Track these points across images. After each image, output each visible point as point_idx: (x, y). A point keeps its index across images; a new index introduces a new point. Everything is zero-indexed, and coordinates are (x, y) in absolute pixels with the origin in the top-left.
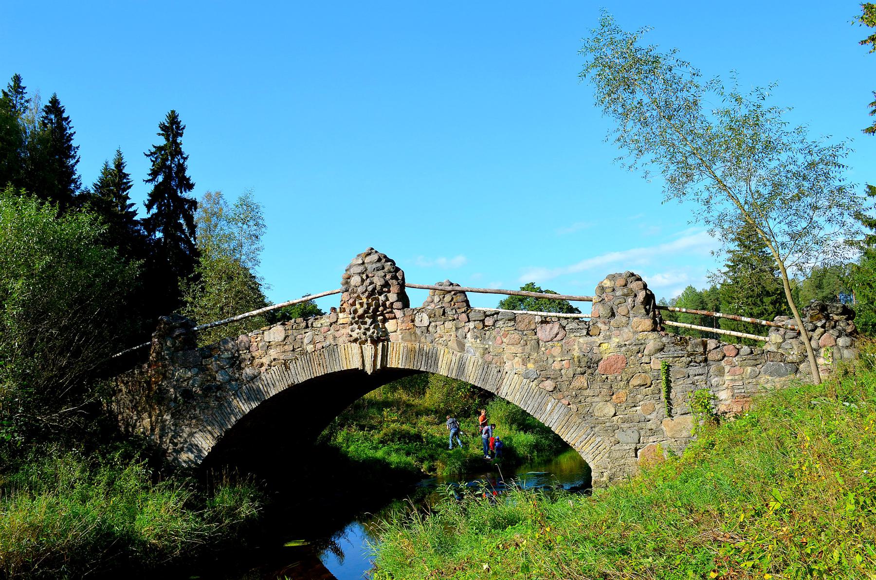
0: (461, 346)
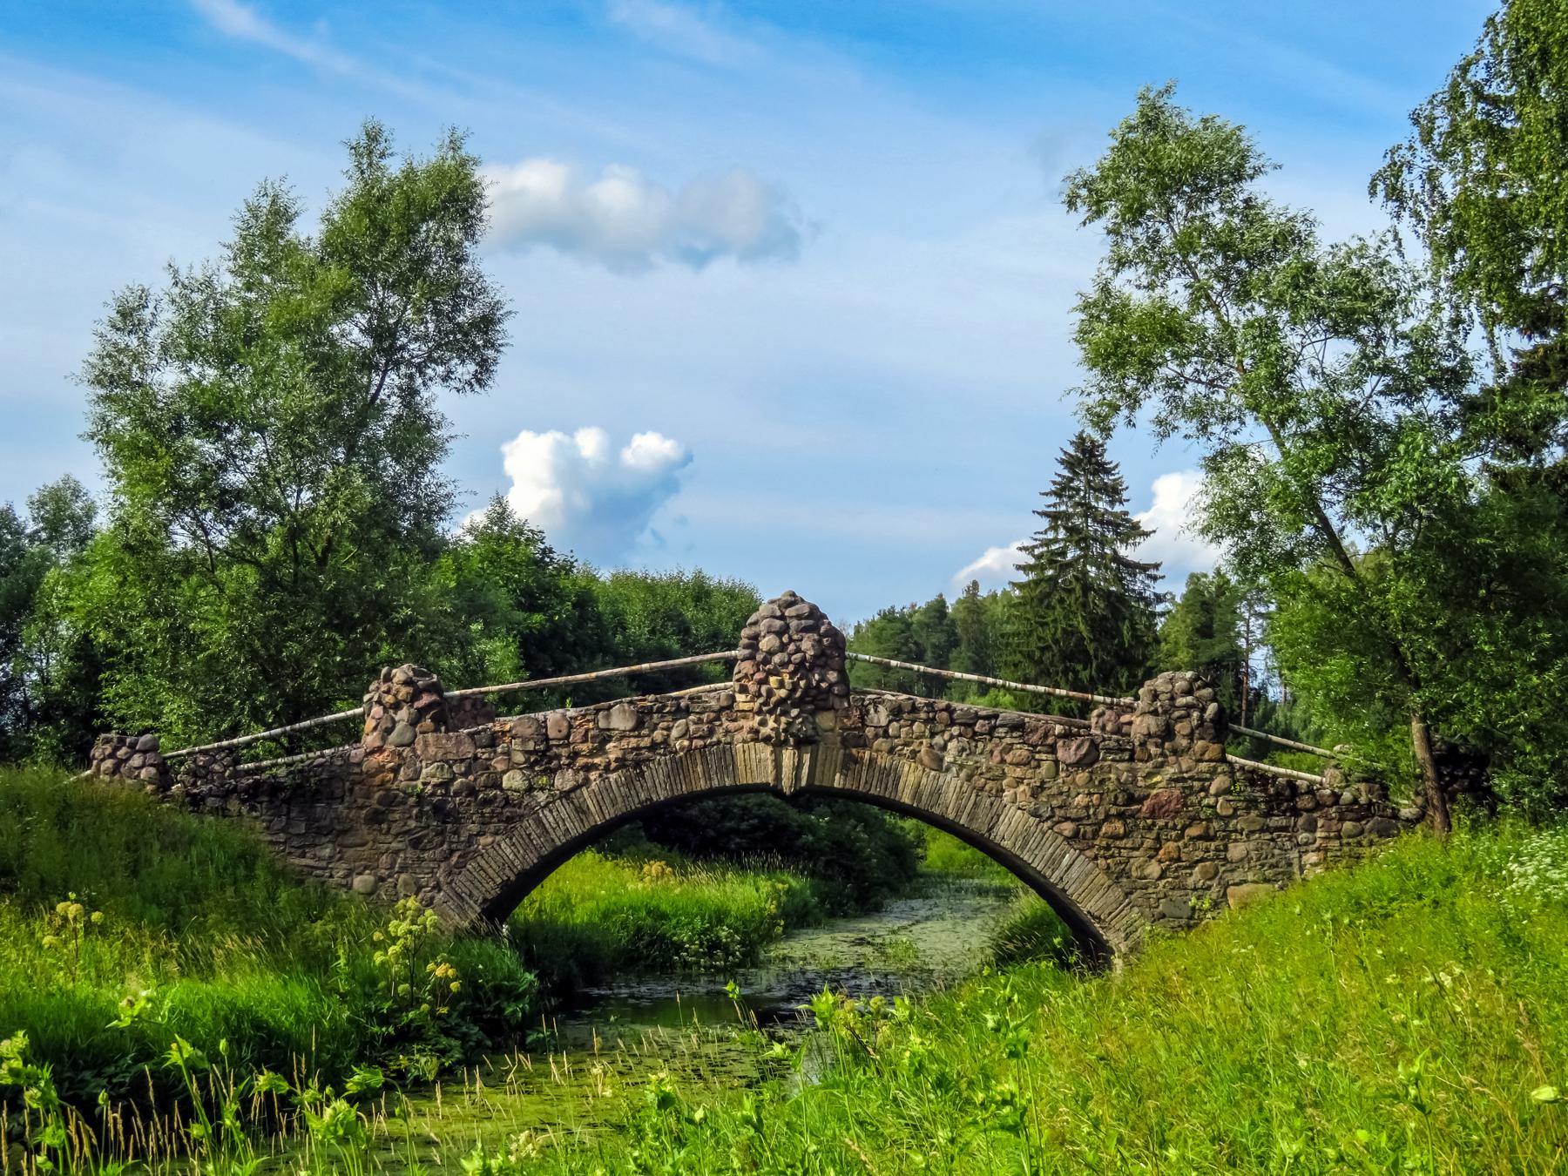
0: (938, 764)
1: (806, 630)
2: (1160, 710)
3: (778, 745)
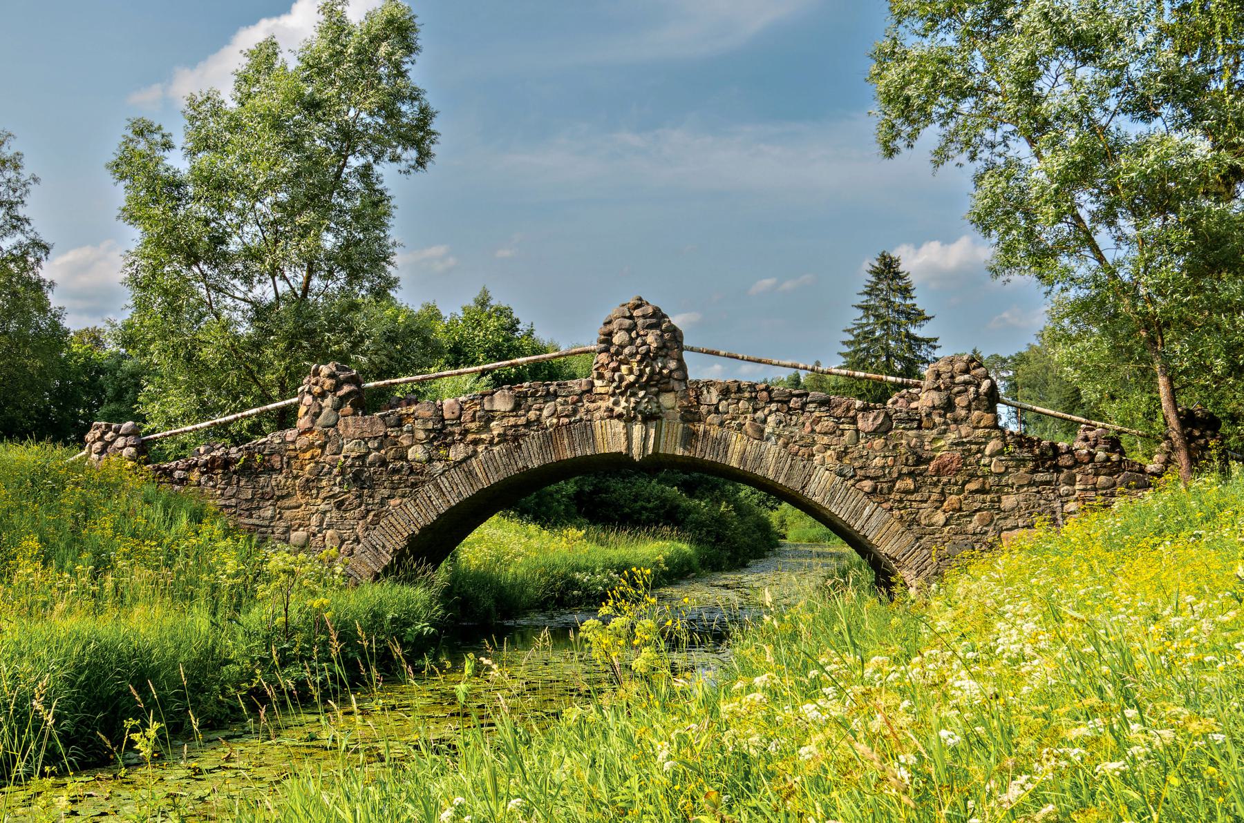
0: (760, 435)
1: (650, 327)
2: (942, 387)
3: (628, 420)
